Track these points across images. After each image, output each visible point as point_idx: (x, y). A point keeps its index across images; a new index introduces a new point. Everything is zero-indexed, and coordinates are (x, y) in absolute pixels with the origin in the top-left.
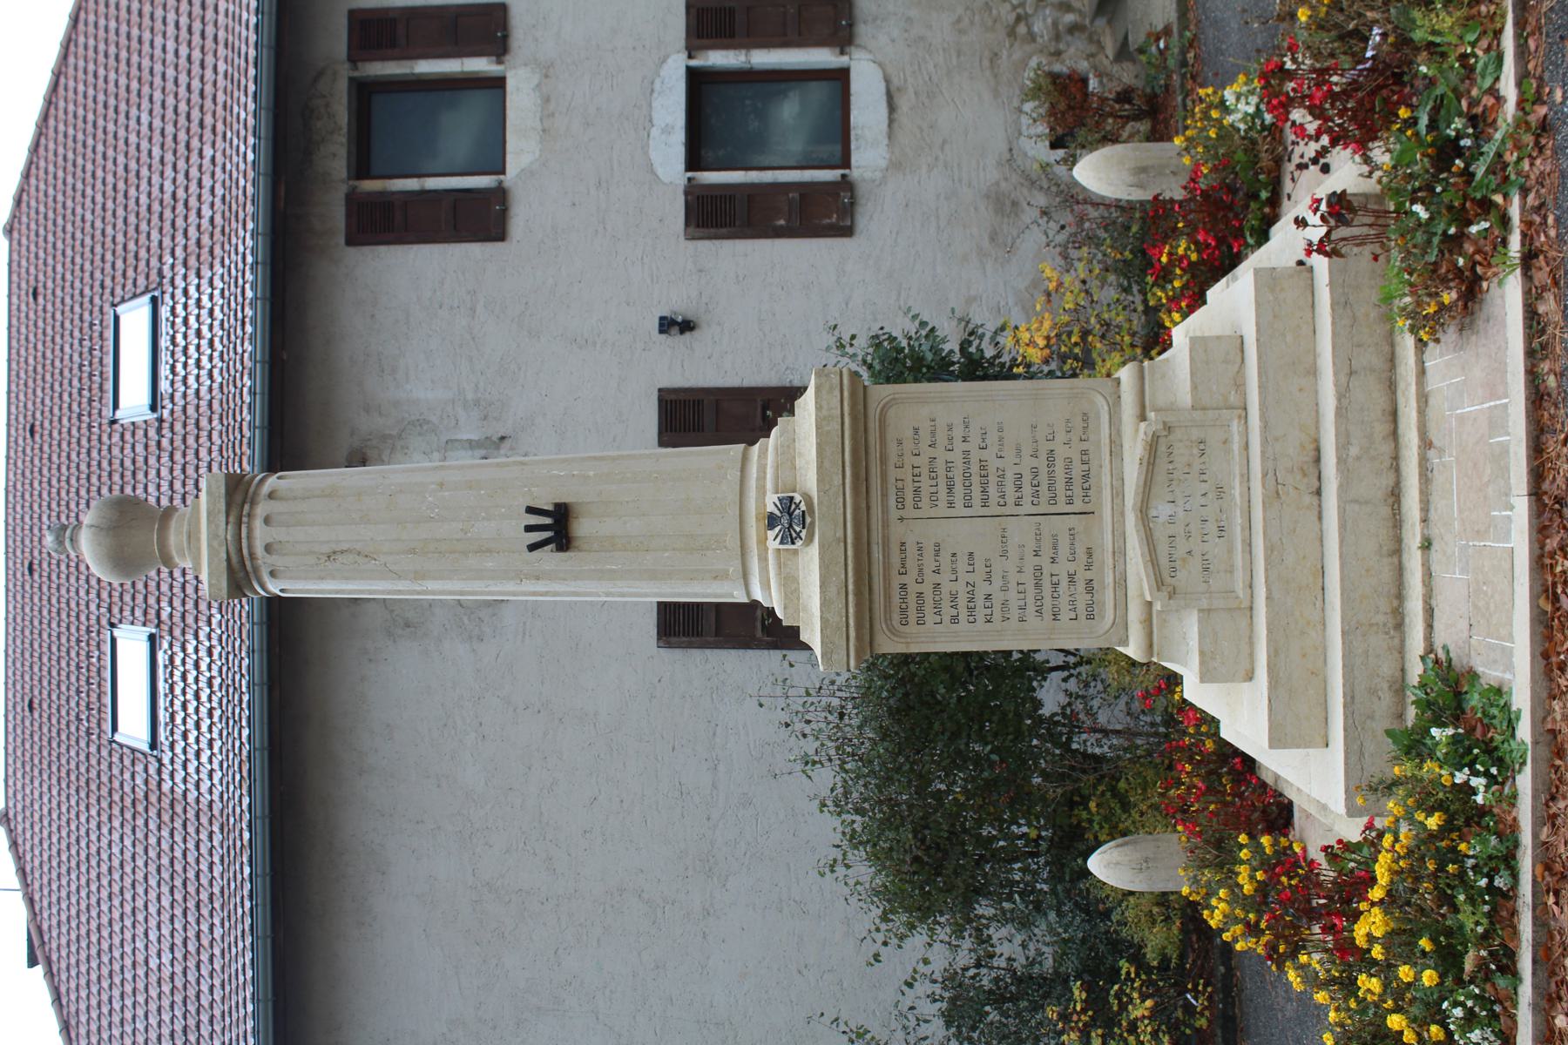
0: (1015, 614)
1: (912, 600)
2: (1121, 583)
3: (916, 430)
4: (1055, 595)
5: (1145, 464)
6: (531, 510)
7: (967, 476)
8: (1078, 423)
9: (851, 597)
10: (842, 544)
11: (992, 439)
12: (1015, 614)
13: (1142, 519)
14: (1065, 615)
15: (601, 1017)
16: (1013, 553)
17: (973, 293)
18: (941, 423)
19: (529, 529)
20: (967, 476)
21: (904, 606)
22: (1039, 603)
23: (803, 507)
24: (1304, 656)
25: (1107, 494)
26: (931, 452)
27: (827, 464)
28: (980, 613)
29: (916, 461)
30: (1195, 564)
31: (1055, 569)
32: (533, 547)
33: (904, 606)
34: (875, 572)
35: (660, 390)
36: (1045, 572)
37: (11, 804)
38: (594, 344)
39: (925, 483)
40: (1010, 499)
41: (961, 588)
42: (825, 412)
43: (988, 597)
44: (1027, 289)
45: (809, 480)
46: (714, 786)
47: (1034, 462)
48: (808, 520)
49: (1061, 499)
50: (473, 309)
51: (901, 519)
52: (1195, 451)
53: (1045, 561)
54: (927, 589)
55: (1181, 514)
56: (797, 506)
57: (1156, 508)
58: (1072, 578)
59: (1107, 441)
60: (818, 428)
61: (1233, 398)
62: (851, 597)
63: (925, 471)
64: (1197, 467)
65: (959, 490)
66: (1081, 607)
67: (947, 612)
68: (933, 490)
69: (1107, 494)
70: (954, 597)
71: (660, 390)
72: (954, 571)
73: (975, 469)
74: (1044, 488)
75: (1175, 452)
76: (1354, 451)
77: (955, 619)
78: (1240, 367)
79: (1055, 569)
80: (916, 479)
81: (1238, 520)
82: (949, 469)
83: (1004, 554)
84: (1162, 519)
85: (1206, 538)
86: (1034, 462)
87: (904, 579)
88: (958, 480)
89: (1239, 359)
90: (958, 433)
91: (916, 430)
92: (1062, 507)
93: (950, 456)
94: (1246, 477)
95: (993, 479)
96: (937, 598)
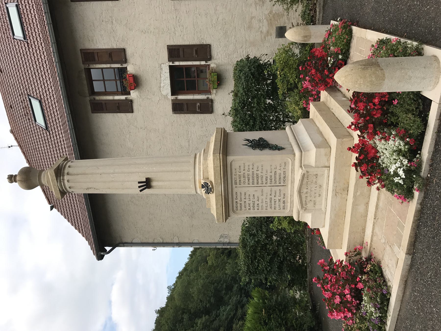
0: (265, 208)
1: (239, 205)
2: (292, 202)
3: (240, 166)
4: (275, 204)
5: (301, 181)
6: (139, 183)
7: (253, 177)
8: (283, 165)
9: (223, 207)
10: (221, 196)
11: (260, 169)
12: (265, 208)
13: (299, 193)
14: (277, 208)
15: (166, 195)
16: (265, 195)
17: (253, 16)
18: (247, 165)
19: (139, 187)
20: (253, 177)
21: (237, 206)
22: (271, 206)
23: (211, 187)
24: (338, 230)
25: (290, 181)
26: (244, 172)
27: (217, 177)
28: (256, 208)
29: (240, 174)
30: (312, 203)
31: (275, 198)
32: (141, 191)
33: (237, 206)
34: (230, 203)
35: (167, 46)
36: (272, 199)
37: (13, 129)
38: (148, 32)
39: (242, 179)
40: (264, 183)
41: (251, 202)
42: (216, 165)
43: (258, 204)
44: (268, 14)
45: (212, 178)
46: (189, 145)
47: (271, 174)
48: (212, 190)
49: (278, 182)
50: (112, 22)
51: (236, 187)
52: (315, 177)
53: (273, 196)
54: (243, 203)
55: (309, 191)
56: (209, 186)
57: (303, 190)
58: (279, 200)
59: (291, 169)
60: (214, 169)
61: (327, 164)
62: (223, 207)
63: (242, 176)
64: (314, 180)
65: (251, 181)
66: (282, 207)
67: (248, 207)
68: (244, 180)
69: (290, 181)
70: (249, 204)
71: (167, 46)
72: (249, 199)
73: (255, 176)
74: (273, 180)
75: (309, 177)
76: (358, 194)
77: (249, 209)
78: (329, 156)
79: (275, 198)
80: (240, 178)
81: (324, 194)
82: (248, 176)
83: (262, 195)
84: (304, 192)
85: (315, 197)
86: (271, 174)
87: (237, 200)
88: (251, 178)
89: (329, 154)
90: (251, 167)
91: (240, 166)
92: (278, 184)
93: (249, 173)
94: (328, 184)
95: (260, 178)
96: (245, 204)
